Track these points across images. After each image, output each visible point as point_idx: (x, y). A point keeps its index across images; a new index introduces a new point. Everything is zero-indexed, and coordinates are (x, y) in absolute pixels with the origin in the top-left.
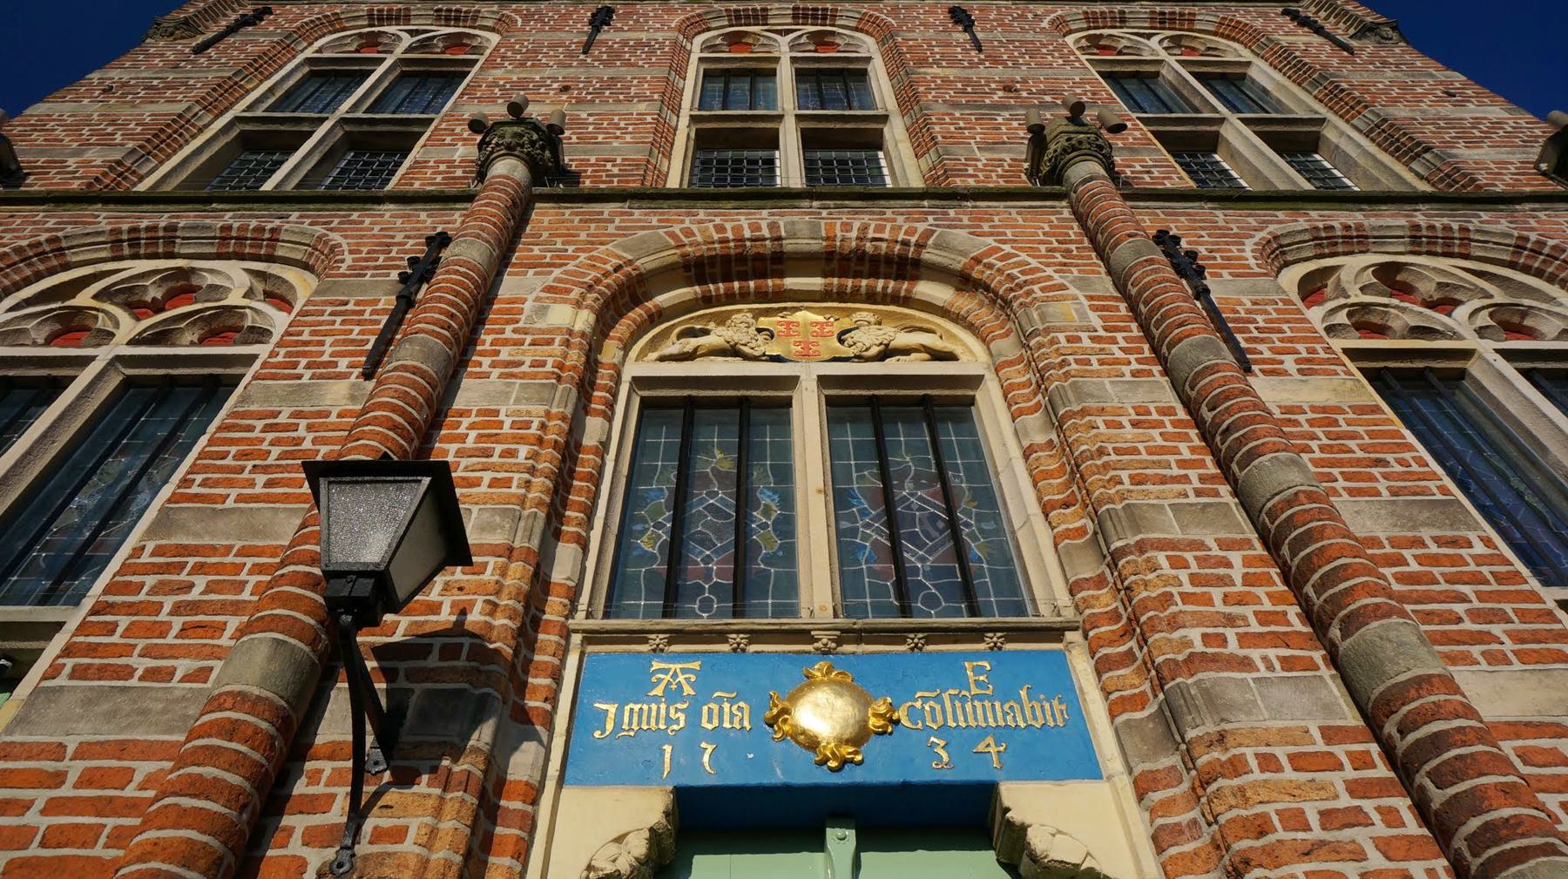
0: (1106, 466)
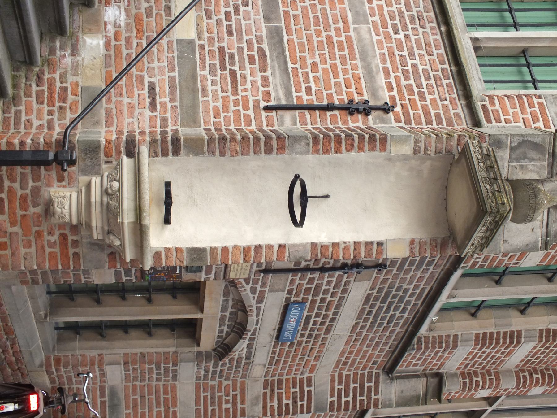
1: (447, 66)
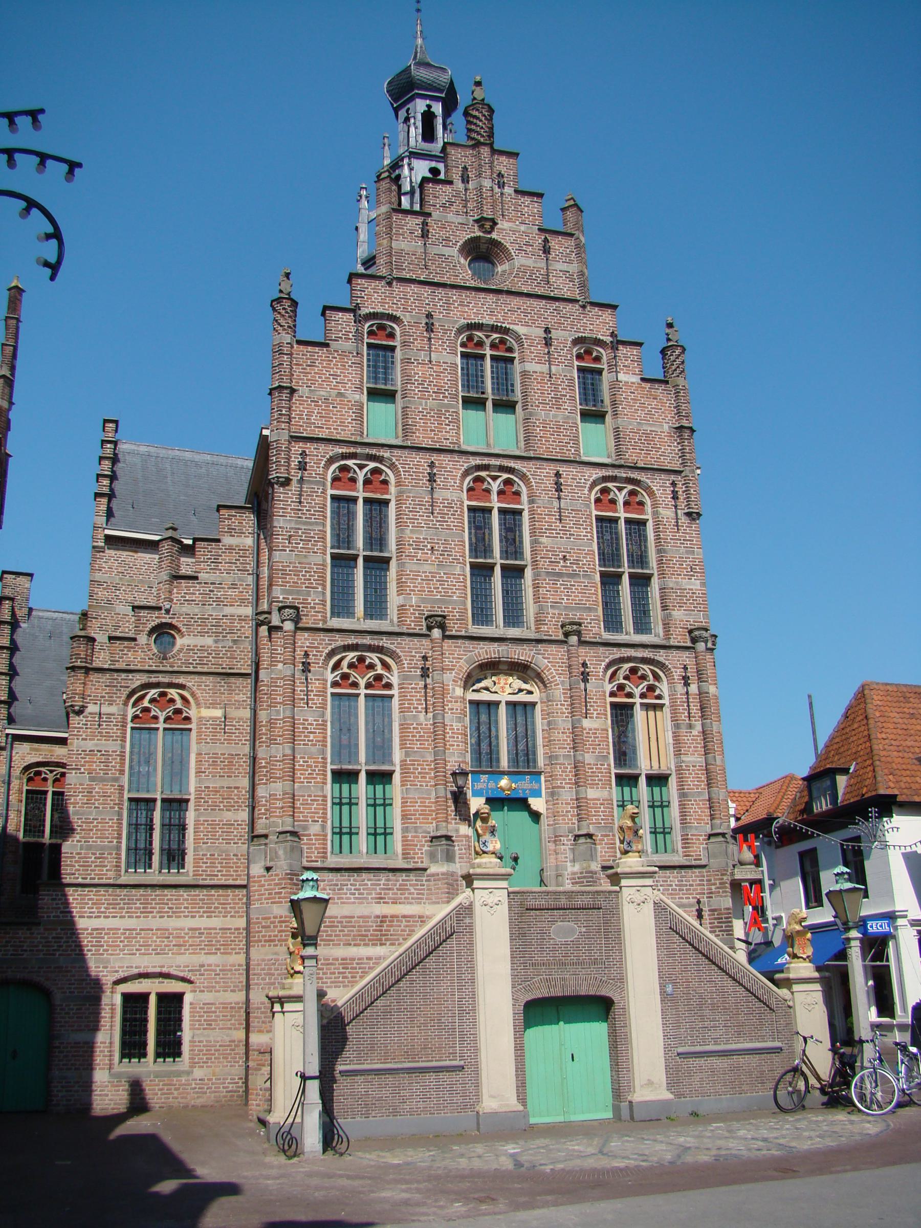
0: (554, 744)
1: (675, 871)
